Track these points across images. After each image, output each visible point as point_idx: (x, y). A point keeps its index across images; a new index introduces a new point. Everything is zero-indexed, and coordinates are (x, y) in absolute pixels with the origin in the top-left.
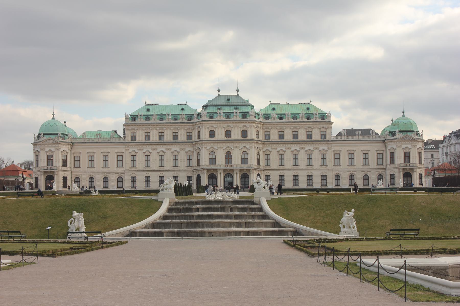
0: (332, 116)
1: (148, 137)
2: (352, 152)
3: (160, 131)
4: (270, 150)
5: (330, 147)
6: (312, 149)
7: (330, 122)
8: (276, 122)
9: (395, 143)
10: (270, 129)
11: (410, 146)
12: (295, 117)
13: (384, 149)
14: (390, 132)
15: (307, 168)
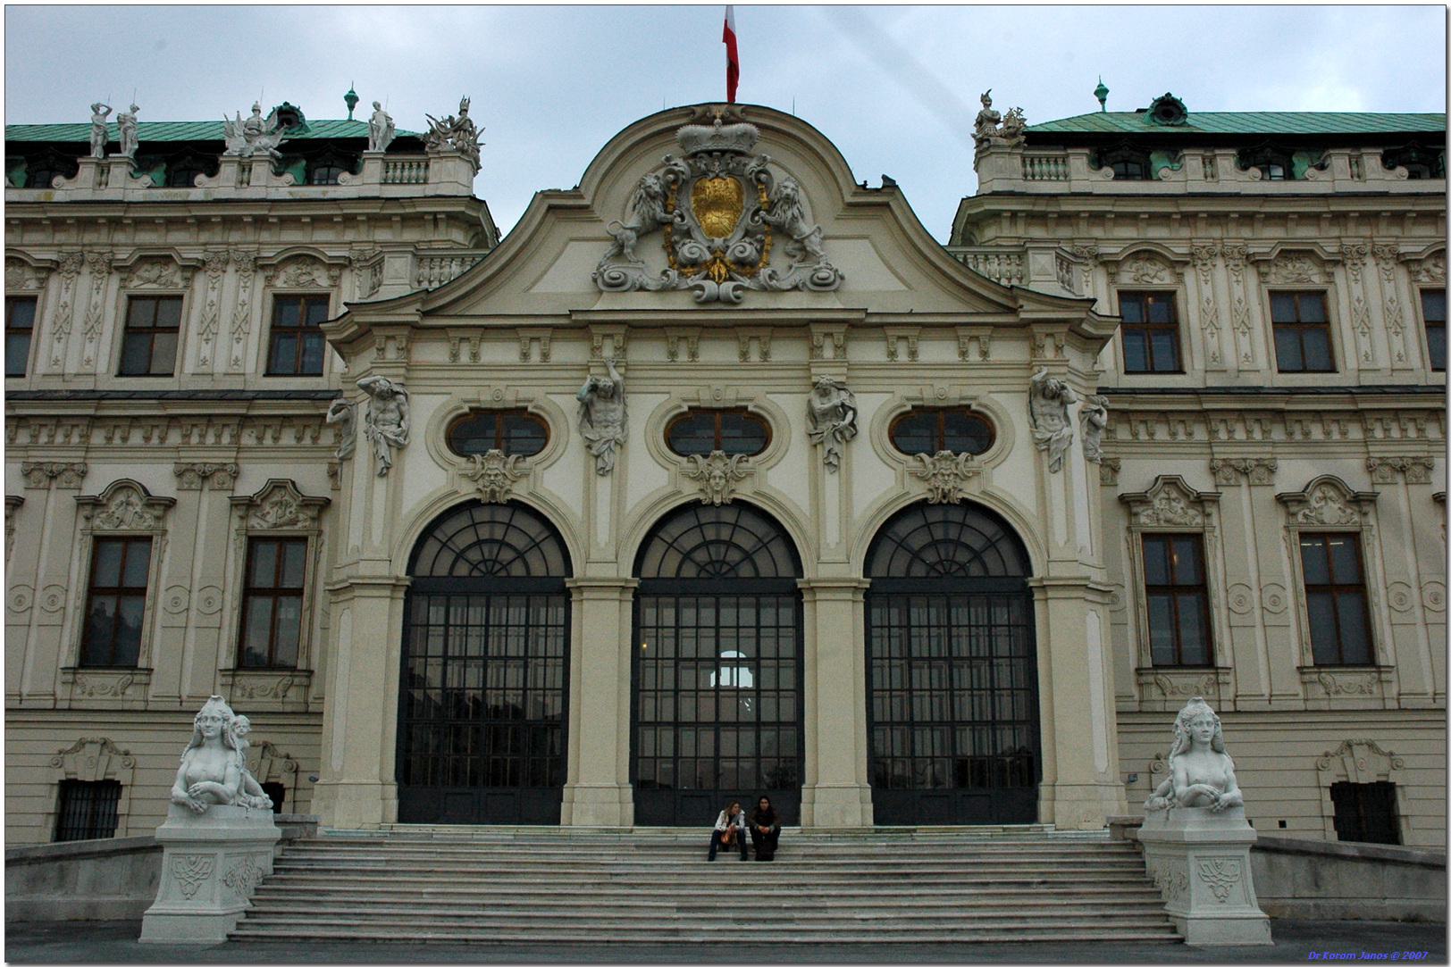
10: (1177, 265)
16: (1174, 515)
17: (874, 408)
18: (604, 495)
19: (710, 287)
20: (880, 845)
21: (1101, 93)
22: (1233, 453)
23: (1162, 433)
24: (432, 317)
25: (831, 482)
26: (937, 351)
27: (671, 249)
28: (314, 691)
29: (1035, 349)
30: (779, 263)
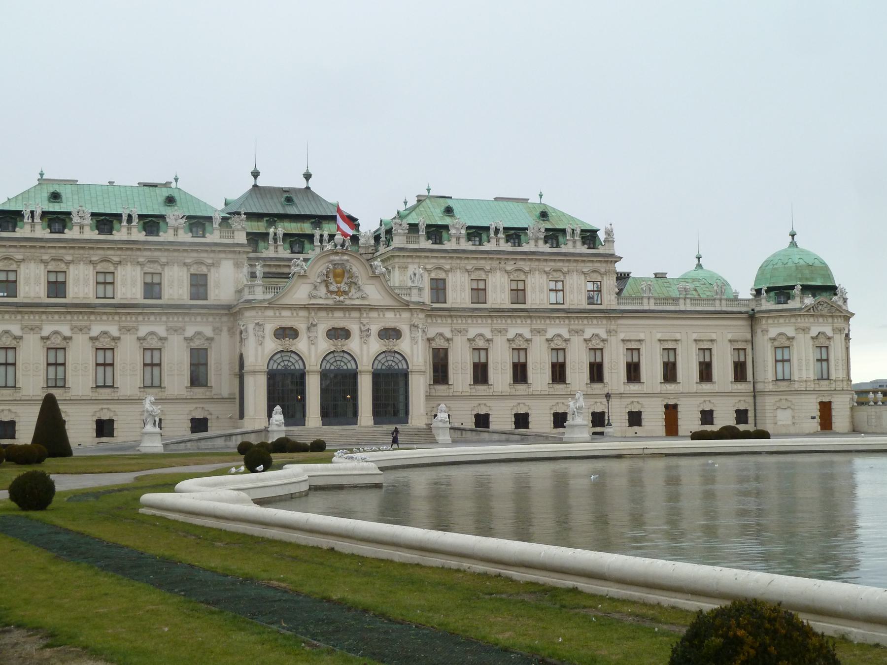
0: (616, 237)
1: (57, 288)
2: (670, 345)
3: (99, 268)
4: (448, 335)
5: (612, 327)
6: (566, 336)
7: (612, 255)
8: (464, 251)
9: (793, 320)
10: (446, 272)
11: (829, 331)
12: (515, 234)
13: (749, 337)
14: (769, 290)
15: (552, 391)
16: (440, 343)
17: (375, 328)
18: (313, 351)
19: (337, 297)
20: (375, 429)
21: (429, 190)
22: (458, 327)
23: (439, 321)
24: (271, 305)
25: (365, 346)
26: (390, 315)
27: (327, 287)
28: (213, 392)
29: (412, 314)
30: (353, 291)
